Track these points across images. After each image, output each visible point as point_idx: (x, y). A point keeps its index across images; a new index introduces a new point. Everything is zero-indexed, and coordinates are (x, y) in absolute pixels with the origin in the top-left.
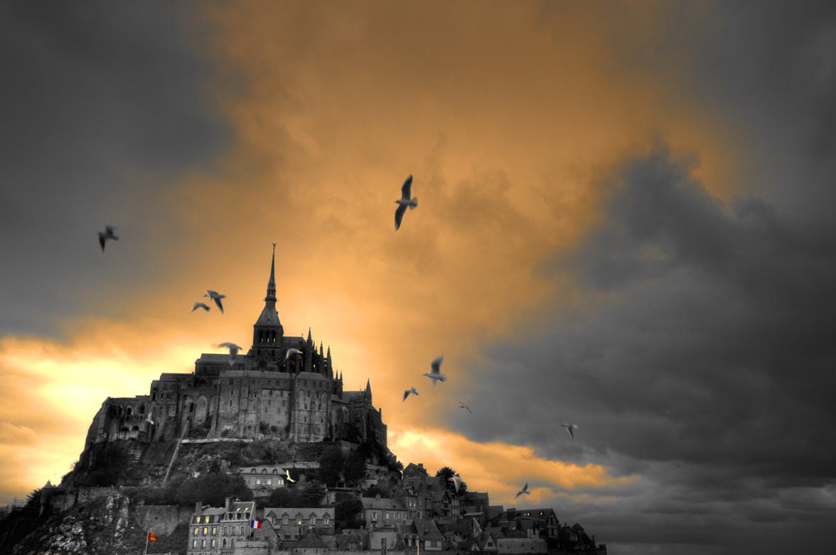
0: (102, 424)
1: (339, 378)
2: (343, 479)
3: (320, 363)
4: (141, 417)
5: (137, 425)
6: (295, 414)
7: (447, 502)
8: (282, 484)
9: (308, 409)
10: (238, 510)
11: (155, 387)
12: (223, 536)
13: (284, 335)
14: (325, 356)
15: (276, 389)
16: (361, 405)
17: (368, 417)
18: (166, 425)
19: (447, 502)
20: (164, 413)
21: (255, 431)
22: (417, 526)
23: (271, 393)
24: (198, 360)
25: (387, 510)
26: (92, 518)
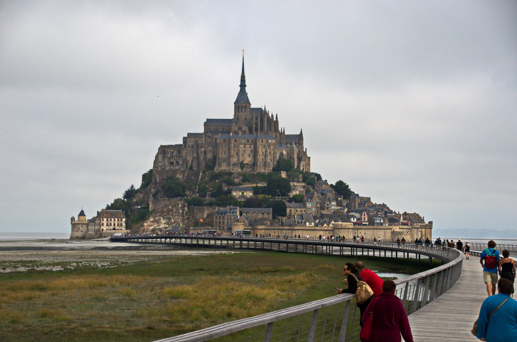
0: (160, 159)
1: (283, 132)
2: (279, 193)
3: (273, 123)
6: (257, 158)
7: (329, 203)
8: (251, 195)
9: (264, 154)
10: (232, 210)
12: (227, 220)
13: (252, 107)
14: (275, 119)
17: (298, 155)
18: (192, 160)
19: (329, 203)
21: (238, 166)
22: (304, 217)
23: (245, 147)
24: (205, 122)
25: (296, 208)
26: (174, 211)
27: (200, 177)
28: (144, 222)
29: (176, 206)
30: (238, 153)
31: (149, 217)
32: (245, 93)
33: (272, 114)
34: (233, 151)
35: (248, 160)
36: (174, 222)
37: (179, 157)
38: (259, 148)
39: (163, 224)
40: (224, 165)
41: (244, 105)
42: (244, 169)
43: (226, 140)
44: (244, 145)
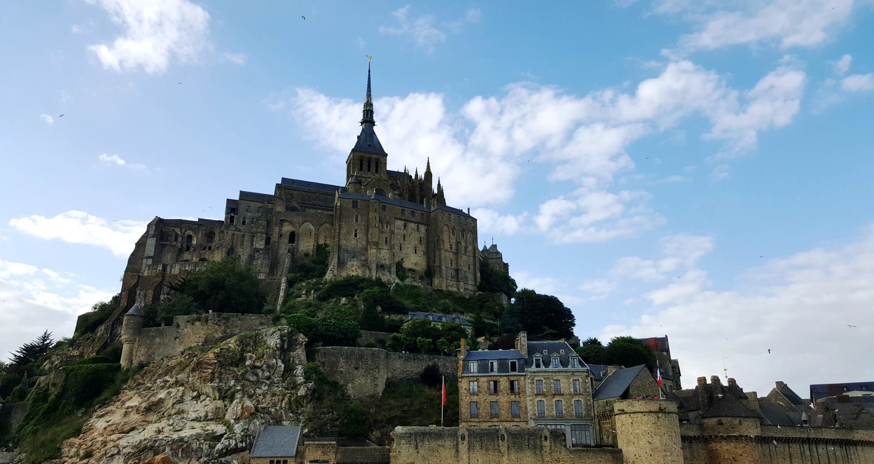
0: (150, 250)
4: (210, 248)
5: (206, 257)
6: (440, 255)
9: (454, 250)
11: (232, 207)
12: (536, 395)
15: (411, 222)
16: (499, 256)
18: (252, 258)
20: (247, 243)
21: (390, 272)
26: (248, 363)
27: (282, 294)
28: (88, 414)
29: (253, 342)
30: (390, 239)
31: (117, 393)
32: (374, 136)
33: (439, 182)
34: (379, 232)
35: (413, 262)
36: (257, 409)
37: (207, 248)
38: (442, 232)
39: (197, 420)
40: (353, 265)
41: (374, 156)
42: (408, 281)
43: (359, 204)
44: (403, 222)
